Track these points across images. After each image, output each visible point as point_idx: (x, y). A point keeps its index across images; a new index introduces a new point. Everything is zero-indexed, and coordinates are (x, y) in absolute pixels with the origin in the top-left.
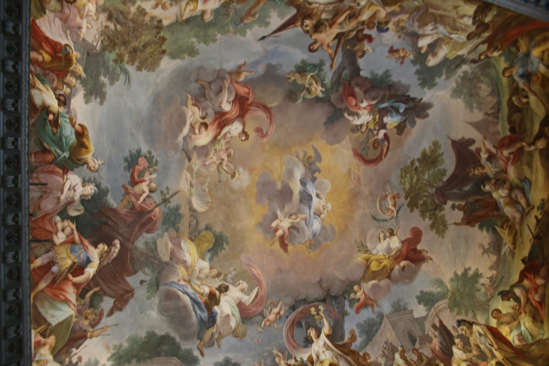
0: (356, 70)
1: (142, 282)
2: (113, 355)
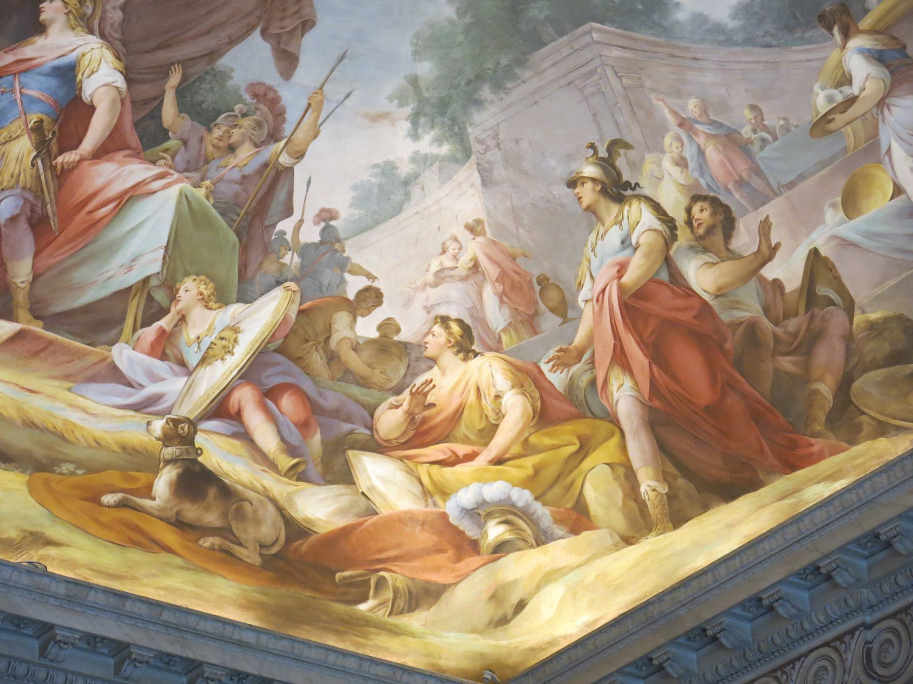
2: (414, 119)
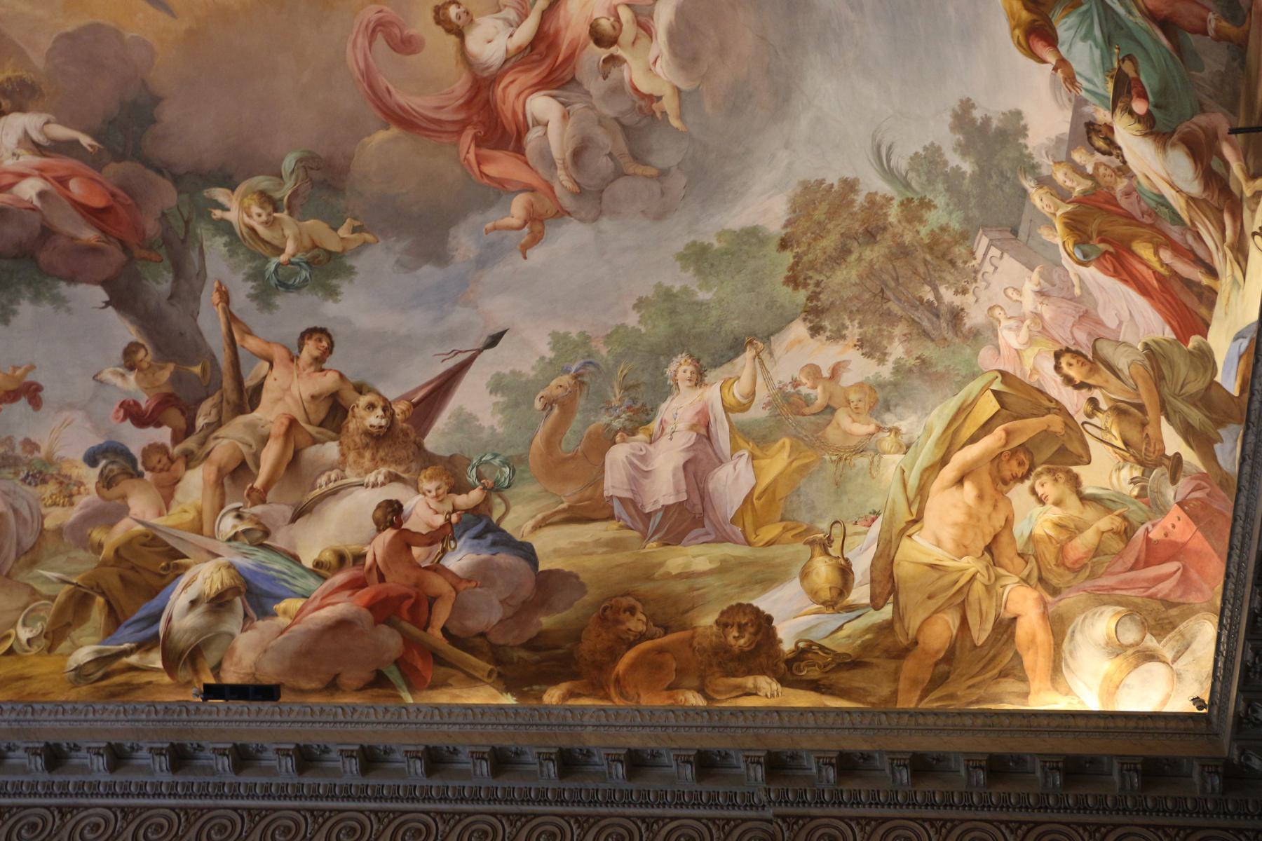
0: (124, 297)
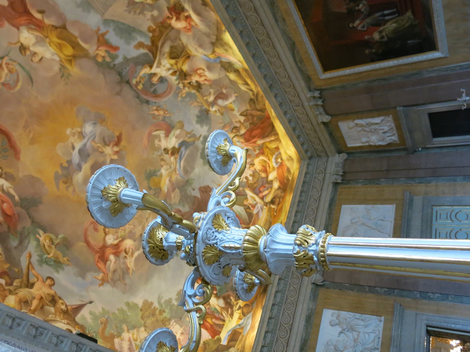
1: (194, 190)
